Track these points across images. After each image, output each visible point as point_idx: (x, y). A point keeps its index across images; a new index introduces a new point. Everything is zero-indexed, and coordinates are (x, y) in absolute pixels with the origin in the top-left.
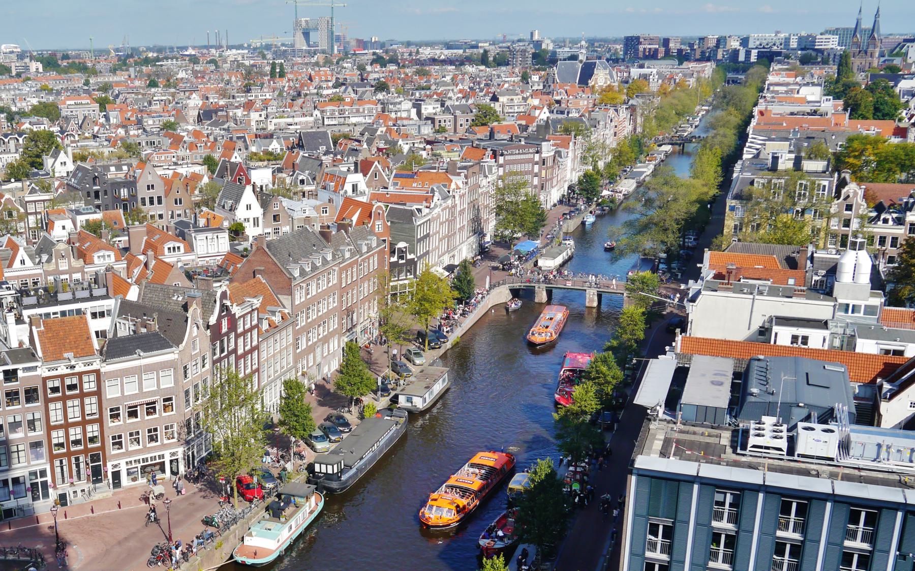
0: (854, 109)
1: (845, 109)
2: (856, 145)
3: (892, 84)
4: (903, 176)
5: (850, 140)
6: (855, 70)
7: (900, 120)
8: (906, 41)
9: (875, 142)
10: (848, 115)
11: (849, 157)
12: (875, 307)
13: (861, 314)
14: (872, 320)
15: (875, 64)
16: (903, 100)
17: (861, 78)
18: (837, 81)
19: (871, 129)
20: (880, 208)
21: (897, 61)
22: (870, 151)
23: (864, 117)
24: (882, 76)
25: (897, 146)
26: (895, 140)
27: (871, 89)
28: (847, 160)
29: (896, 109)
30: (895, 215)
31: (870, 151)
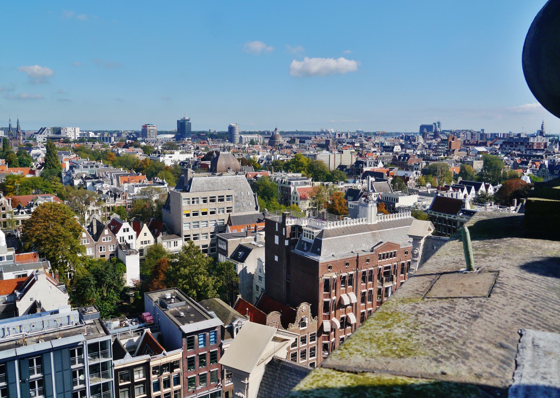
0: (10, 163)
1: (6, 163)
2: (10, 179)
3: (28, 151)
4: (34, 191)
5: (7, 177)
6: (13, 146)
7: (32, 167)
8: (35, 133)
9: (18, 177)
10: (7, 166)
11: (8, 185)
12: (11, 256)
13: (6, 260)
14: (11, 262)
15: (21, 143)
16: (34, 158)
17: (15, 150)
18: (3, 151)
19: (17, 172)
20: (19, 208)
21: (31, 142)
22: (17, 181)
23: (16, 167)
24: (24, 148)
25: (30, 179)
26: (29, 176)
27: (18, 155)
28: (7, 186)
29: (30, 162)
30: (26, 210)
31: (17, 181)
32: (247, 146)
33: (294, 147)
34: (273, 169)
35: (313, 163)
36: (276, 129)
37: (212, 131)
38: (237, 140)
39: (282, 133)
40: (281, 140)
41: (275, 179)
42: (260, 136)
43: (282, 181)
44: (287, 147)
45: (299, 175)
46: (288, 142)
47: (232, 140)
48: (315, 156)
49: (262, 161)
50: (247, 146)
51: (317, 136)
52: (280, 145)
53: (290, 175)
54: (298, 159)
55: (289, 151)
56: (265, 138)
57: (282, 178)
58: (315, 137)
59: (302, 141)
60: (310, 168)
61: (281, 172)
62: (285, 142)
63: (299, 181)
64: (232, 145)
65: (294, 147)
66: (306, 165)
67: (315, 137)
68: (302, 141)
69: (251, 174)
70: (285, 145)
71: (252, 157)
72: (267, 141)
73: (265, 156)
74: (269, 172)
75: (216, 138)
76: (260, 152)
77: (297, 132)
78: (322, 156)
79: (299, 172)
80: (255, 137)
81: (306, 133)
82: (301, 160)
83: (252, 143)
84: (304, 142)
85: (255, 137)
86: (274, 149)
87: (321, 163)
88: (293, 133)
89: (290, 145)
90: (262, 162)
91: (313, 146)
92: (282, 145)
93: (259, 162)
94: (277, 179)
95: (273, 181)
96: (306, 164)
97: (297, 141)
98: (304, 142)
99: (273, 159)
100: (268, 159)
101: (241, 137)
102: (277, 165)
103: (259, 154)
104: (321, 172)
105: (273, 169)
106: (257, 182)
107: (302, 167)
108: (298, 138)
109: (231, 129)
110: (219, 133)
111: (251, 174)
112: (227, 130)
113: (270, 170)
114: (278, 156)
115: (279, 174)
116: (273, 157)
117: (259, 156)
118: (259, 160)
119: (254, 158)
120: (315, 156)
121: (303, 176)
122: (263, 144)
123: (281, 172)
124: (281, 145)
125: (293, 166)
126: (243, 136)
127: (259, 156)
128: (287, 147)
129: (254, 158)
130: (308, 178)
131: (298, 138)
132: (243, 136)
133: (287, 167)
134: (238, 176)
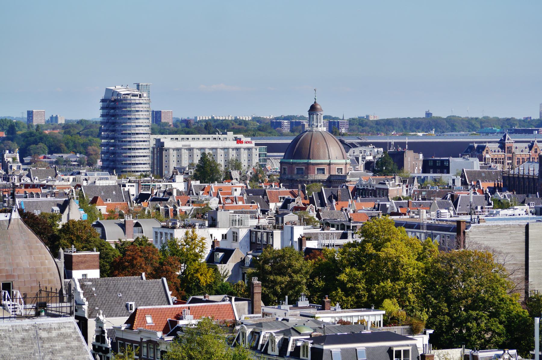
32: (179, 184)
33: (396, 188)
34: (258, 291)
35: (450, 261)
36: (313, 109)
37: (37, 121)
38: (142, 161)
39: (333, 126)
40: (333, 157)
41: (255, 335)
42: (248, 142)
43: (285, 343)
44: (360, 192)
45: (373, 317)
46: (368, 166)
47: (115, 163)
48: (458, 229)
49: (228, 253)
50: (179, 184)
51: (510, 140)
52: (330, 182)
53: (328, 317)
54: (378, 247)
55: (363, 208)
56: (272, 148)
57: (287, 332)
58: (502, 145)
59: (435, 164)
60: (430, 287)
61: (293, 302)
62: (361, 166)
63: (361, 347)
64: (112, 181)
65: (396, 188)
66: (412, 272)
67: (502, 145)
68: (435, 164)
69: (154, 313)
70: (352, 183)
71: (179, 234)
72: (274, 165)
73: (243, 233)
74: (239, 309)
75: (54, 149)
76: (222, 216)
77: (409, 125)
78: (489, 231)
79: (375, 303)
80: (221, 145)
81: (470, 125)
82: (389, 251)
83: (206, 171)
84: (444, 168)
85: (221, 145)
86: (299, 201)
87: (485, 259)
88: (386, 125)
89: (370, 179)
90: (224, 260)
91: (485, 185)
92: (340, 180)
93: (211, 259)
94: (265, 334)
95: (244, 345)
96: (411, 265)
97: (413, 163)
98: (444, 168)
99: (277, 245)
100: (256, 242)
101: (160, 147)
102: (281, 271)
103: (213, 224)
104: (478, 303)
105: (258, 291)
106: (170, 350)
107: (395, 280)
108: (416, 147)
109: (115, 108)
110: (67, 128)
111: (154, 313)
112: (94, 113)
113: (247, 295)
114: (299, 231)
115: (283, 311)
116: (277, 234)
117: (217, 233)
118: (215, 249)
119: (190, 240)
120: (458, 229)
121: (390, 320)
122: (255, 178)
123: (293, 302)
124: (335, 181)
125: (353, 279)
126: (168, 142)
127: (217, 233)
128: (360, 192)
129: (190, 240)
130: (414, 331)
131: (416, 147)
132: (168, 142)
133: (326, 281)
134: (44, 321)
